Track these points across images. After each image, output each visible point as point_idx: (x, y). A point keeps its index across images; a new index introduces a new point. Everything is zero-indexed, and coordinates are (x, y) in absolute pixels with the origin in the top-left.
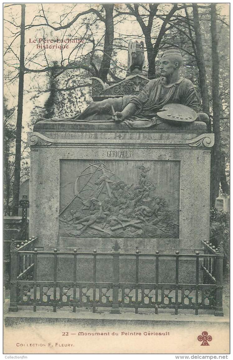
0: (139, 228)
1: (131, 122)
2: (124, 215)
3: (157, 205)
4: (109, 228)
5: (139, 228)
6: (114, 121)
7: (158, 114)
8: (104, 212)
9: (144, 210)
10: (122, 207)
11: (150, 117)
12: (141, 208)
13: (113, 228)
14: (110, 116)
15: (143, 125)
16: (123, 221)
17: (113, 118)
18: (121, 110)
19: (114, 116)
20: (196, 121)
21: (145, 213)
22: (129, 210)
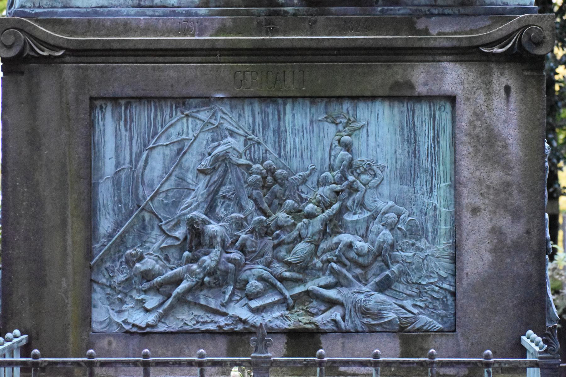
0: (331, 303)
2: (288, 264)
3: (386, 232)
4: (243, 301)
5: (331, 303)
8: (228, 255)
9: (350, 246)
10: (283, 237)
12: (337, 244)
13: (254, 304)
16: (282, 279)
21: (352, 254)
22: (302, 247)
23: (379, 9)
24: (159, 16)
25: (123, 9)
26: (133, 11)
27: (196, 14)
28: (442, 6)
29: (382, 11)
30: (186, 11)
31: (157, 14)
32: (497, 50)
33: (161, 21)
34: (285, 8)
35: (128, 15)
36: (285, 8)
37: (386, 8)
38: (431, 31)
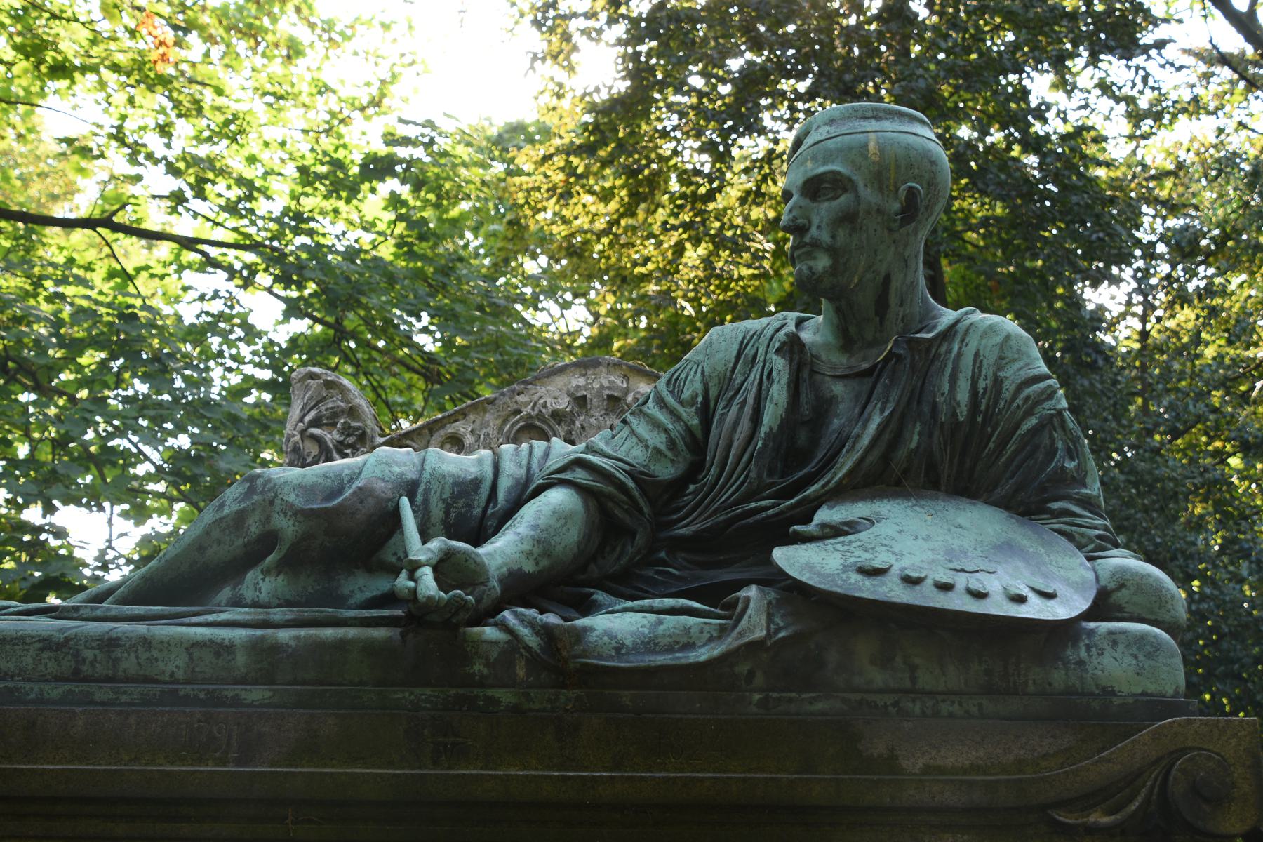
1: (552, 619)
6: (417, 615)
7: (782, 556)
11: (719, 598)
14: (381, 585)
15: (649, 644)
17: (403, 582)
18: (478, 538)
19: (414, 567)
20: (1088, 615)
23: (757, 697)
24: (130, 704)
25: (28, 686)
26: (55, 691)
27: (236, 702)
28: (931, 694)
29: (764, 703)
30: (208, 692)
31: (124, 698)
32: (1098, 818)
33: (132, 720)
34: (490, 692)
35: (40, 701)
36: (490, 692)
37: (775, 695)
38: (905, 763)
